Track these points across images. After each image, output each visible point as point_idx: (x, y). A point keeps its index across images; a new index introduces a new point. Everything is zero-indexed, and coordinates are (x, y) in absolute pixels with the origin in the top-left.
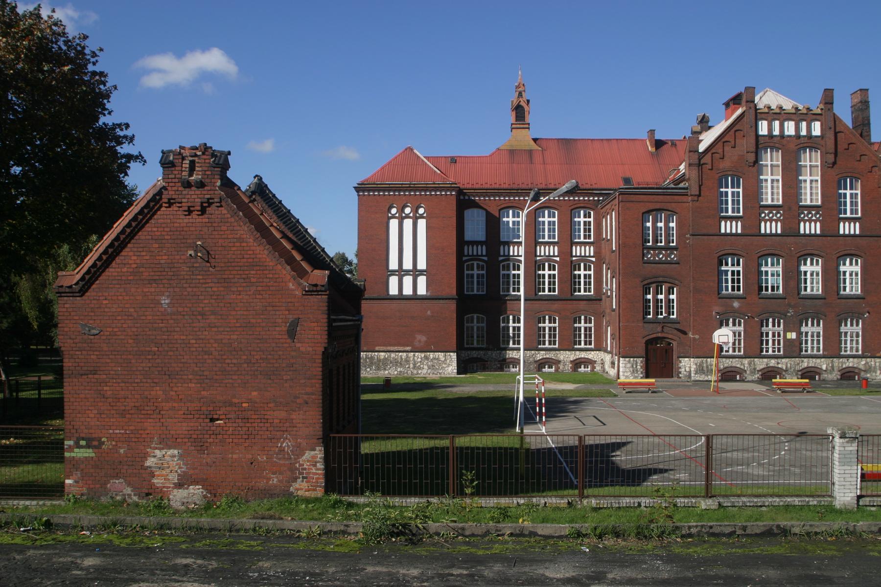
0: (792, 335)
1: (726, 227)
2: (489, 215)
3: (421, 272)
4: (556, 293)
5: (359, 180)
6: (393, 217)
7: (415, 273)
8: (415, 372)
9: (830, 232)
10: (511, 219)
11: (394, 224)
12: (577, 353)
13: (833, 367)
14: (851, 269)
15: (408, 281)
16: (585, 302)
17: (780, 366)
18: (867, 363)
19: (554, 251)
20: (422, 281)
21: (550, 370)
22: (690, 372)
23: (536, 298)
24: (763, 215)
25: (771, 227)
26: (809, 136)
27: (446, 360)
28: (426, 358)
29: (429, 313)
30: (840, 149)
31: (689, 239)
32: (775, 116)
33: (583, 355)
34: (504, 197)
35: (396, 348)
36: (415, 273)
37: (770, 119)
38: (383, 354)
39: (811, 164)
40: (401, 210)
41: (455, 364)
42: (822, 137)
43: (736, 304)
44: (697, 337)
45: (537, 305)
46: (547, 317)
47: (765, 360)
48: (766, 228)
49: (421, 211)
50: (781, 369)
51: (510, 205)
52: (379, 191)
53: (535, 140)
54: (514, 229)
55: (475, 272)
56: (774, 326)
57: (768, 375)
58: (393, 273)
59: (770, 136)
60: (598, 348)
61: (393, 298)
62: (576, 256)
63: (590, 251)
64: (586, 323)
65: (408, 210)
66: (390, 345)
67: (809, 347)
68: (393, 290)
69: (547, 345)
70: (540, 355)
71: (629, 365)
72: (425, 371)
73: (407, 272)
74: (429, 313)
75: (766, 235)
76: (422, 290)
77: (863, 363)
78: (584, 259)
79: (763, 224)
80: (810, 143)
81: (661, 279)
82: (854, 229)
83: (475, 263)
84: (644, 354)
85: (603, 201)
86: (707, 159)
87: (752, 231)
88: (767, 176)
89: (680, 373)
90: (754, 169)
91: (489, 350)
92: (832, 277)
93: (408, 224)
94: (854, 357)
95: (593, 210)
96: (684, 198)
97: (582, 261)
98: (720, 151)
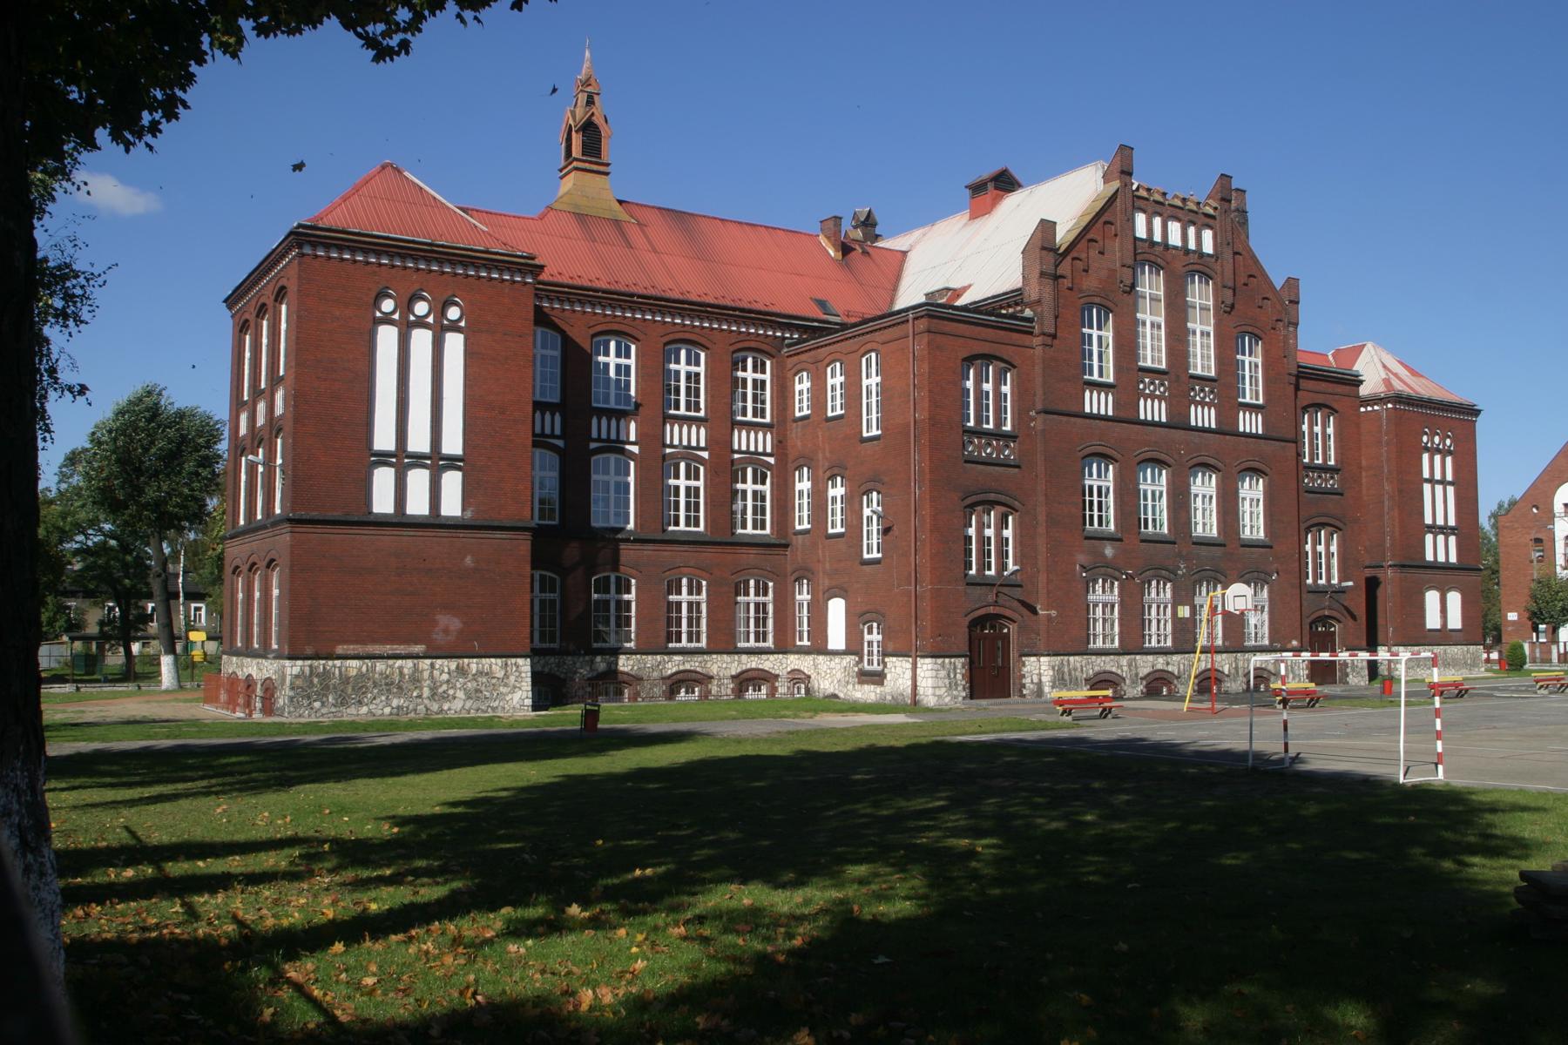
0: (1184, 612)
2: (568, 344)
3: (452, 462)
4: (702, 528)
6: (387, 320)
7: (437, 462)
8: (435, 707)
10: (612, 360)
11: (387, 337)
12: (744, 657)
13: (1236, 668)
15: (418, 479)
16: (754, 551)
17: (1170, 669)
19: (697, 436)
20: (452, 482)
21: (691, 697)
22: (1040, 684)
23: (659, 536)
26: (1199, 253)
27: (506, 676)
28: (461, 671)
29: (468, 560)
31: (1033, 419)
32: (1158, 209)
33: (752, 662)
34: (604, 308)
35: (388, 649)
36: (437, 462)
37: (1150, 210)
38: (354, 663)
40: (407, 305)
41: (527, 684)
42: (1216, 256)
43: (1109, 551)
44: (1053, 613)
45: (667, 554)
46: (684, 581)
47: (1150, 658)
49: (453, 313)
51: (616, 327)
52: (353, 250)
53: (621, 202)
54: (618, 381)
57: (1207, 683)
58: (383, 459)
59: (1150, 241)
60: (783, 648)
61: (382, 522)
62: (740, 452)
63: (763, 442)
64: (757, 594)
65: (421, 308)
66: (374, 641)
68: (383, 503)
69: (684, 643)
70: (673, 665)
71: (943, 673)
72: (457, 705)
73: (418, 460)
74: (468, 560)
76: (452, 505)
78: (753, 458)
80: (1199, 265)
81: (992, 496)
84: (965, 650)
85: (799, 342)
86: (1065, 268)
88: (1145, 316)
89: (1024, 686)
91: (568, 653)
93: (421, 340)
95: (771, 356)
96: (1025, 339)
97: (750, 462)
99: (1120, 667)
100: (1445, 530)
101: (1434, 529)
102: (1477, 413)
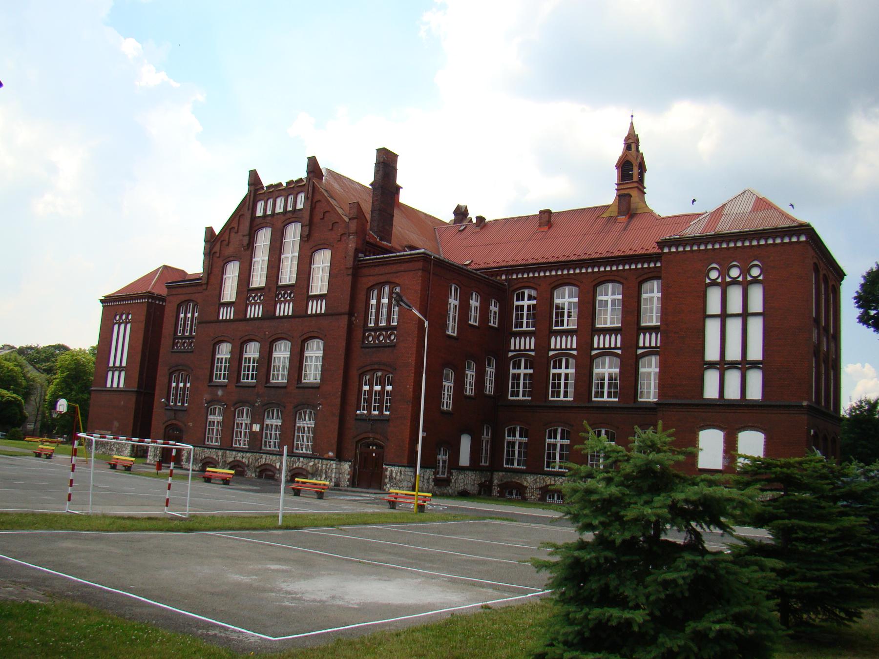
0: (256, 428)
9: (300, 314)
14: (314, 352)
17: (244, 460)
18: (315, 464)
26: (295, 210)
30: (317, 219)
47: (234, 453)
50: (244, 463)
67: (272, 440)
77: (311, 464)
90: (249, 252)
93: (123, 326)
94: (305, 456)
99: (218, 456)
100: (120, 369)
101: (723, 365)
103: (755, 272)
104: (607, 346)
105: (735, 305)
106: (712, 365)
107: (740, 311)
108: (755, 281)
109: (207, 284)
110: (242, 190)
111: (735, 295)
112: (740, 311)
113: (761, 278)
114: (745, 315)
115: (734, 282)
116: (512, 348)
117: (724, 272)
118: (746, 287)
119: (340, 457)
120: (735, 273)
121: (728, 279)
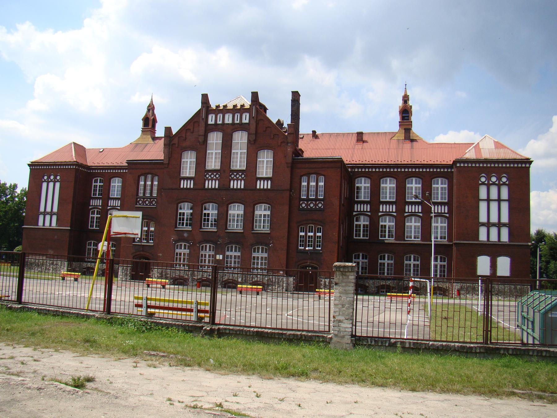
0: (219, 257)
1: (184, 184)
3: (54, 214)
5: (33, 160)
6: (45, 181)
11: (45, 185)
15: (48, 217)
24: (208, 176)
25: (212, 184)
27: (61, 265)
29: (56, 237)
36: (51, 214)
39: (240, 140)
48: (209, 184)
55: (95, 216)
56: (210, 250)
58: (41, 213)
74: (56, 237)
75: (208, 189)
77: (266, 279)
79: (207, 182)
80: (241, 127)
82: (267, 185)
83: (96, 210)
87: (199, 187)
92: (249, 218)
93: (51, 184)
98: (184, 135)
102: (530, 162)
103: (504, 180)
104: (413, 211)
105: (494, 194)
106: (483, 224)
107: (496, 198)
108: (504, 184)
109: (168, 164)
110: (197, 106)
111: (494, 191)
112: (496, 198)
113: (507, 183)
114: (499, 200)
115: (494, 184)
116: (356, 210)
117: (489, 179)
118: (499, 186)
119: (288, 274)
120: (494, 179)
121: (491, 182)
